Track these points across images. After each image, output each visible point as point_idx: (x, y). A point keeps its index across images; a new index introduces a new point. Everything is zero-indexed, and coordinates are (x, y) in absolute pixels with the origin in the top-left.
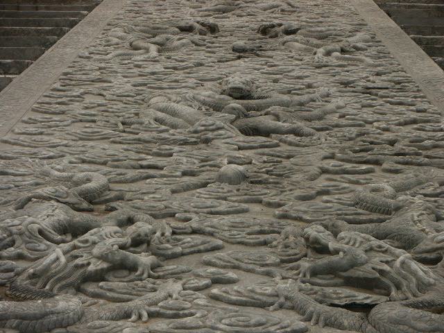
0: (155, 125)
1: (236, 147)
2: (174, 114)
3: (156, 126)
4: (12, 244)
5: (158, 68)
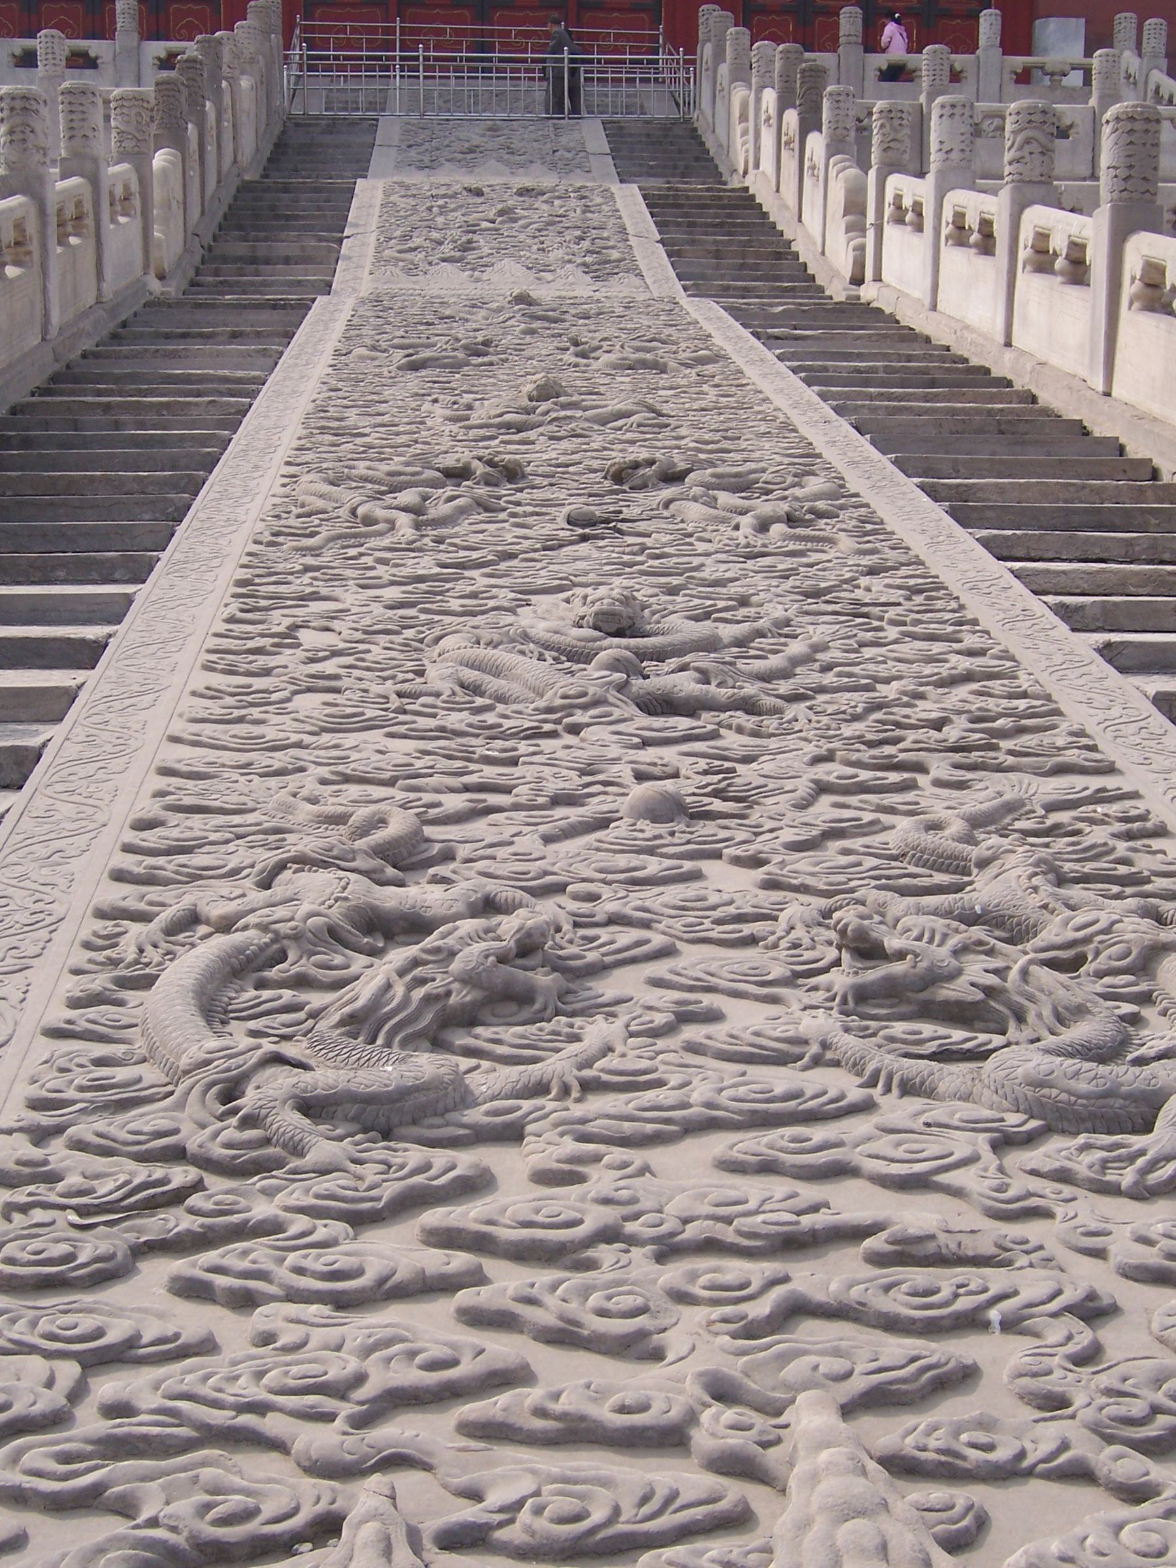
2: (496, 671)
3: (468, 698)
4: (282, 957)
5: (426, 565)
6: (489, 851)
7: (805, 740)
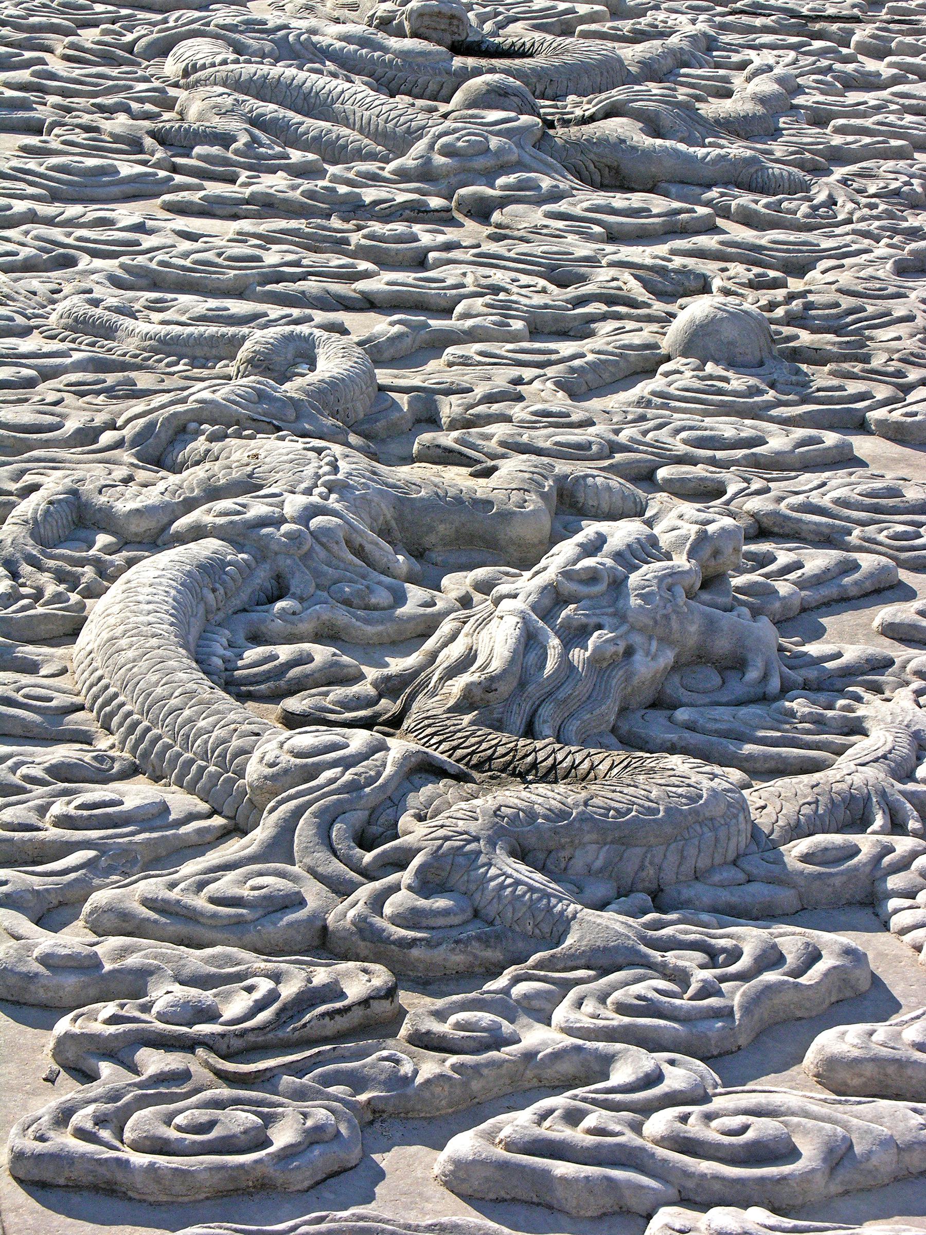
0: (270, 147)
1: (597, 229)
6: (496, 408)
7: (866, 234)
